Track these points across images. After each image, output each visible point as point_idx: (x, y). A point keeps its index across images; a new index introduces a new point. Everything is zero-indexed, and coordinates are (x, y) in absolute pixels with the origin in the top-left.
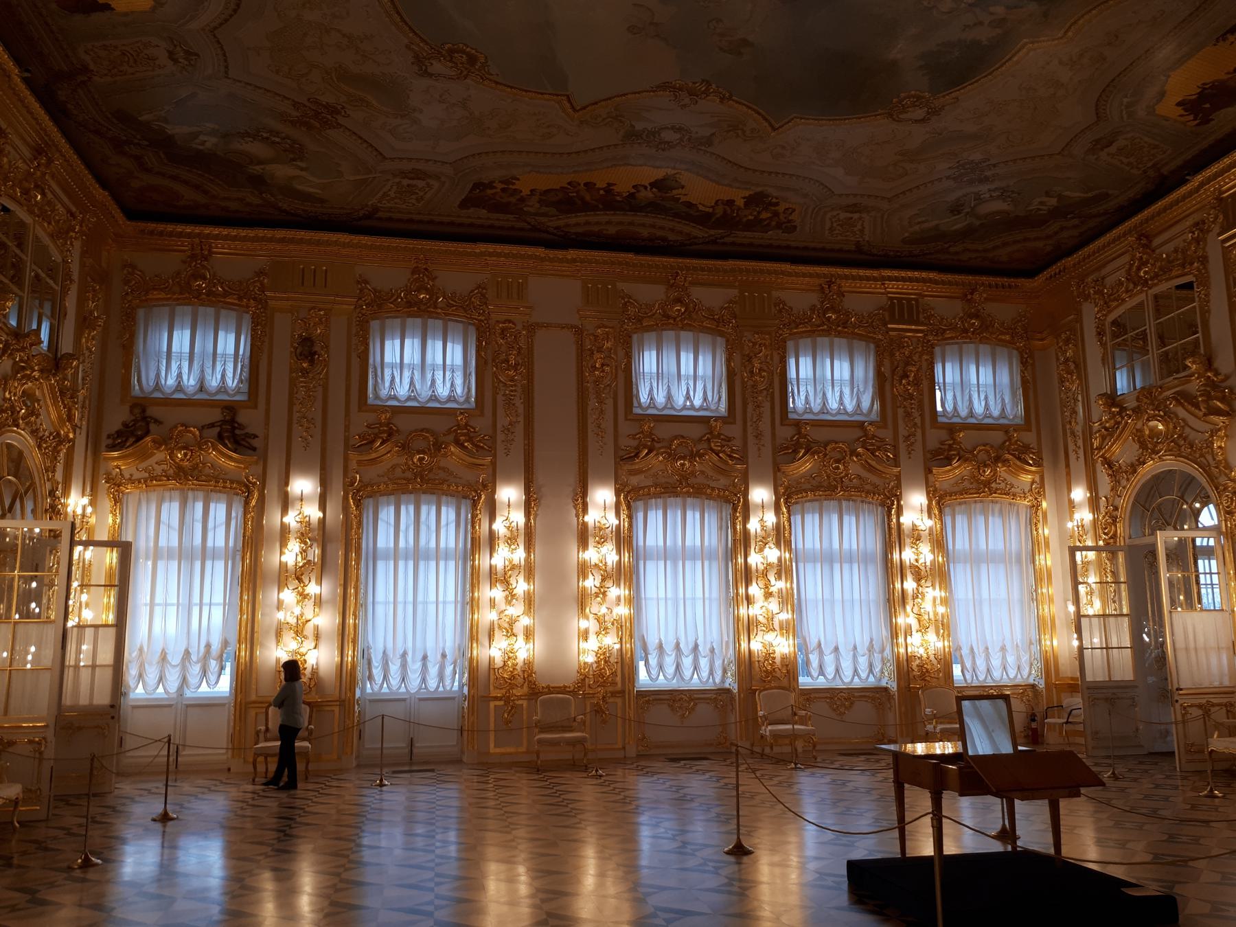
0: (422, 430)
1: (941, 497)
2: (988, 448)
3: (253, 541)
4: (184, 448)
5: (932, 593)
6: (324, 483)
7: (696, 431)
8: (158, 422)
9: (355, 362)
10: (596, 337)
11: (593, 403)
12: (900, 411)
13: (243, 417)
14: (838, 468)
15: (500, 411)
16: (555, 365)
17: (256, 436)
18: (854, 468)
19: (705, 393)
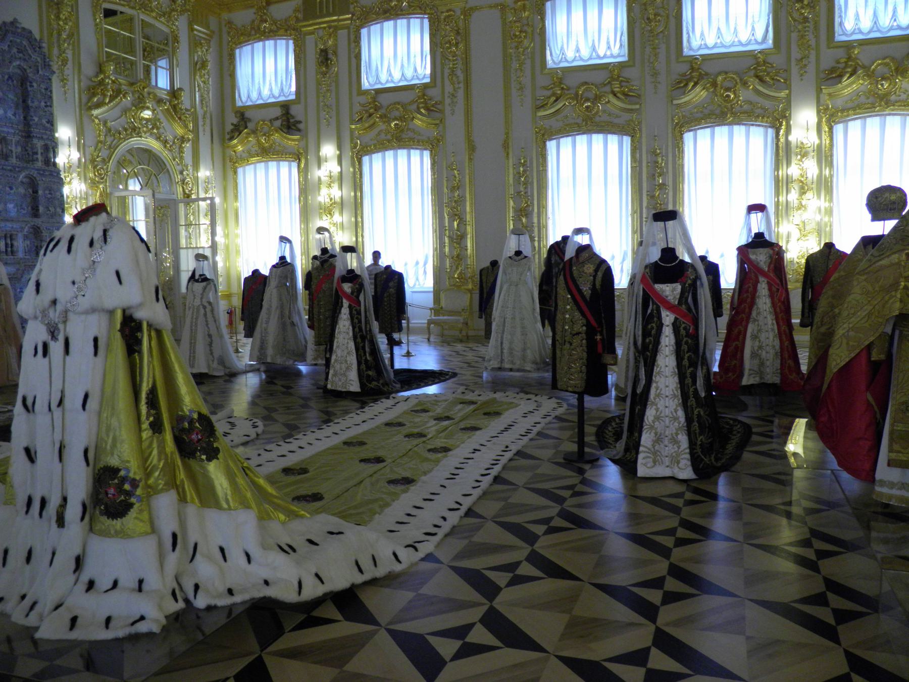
0: (395, 104)
1: (832, 115)
2: (887, 60)
3: (306, 189)
4: (264, 135)
5: (814, 202)
6: (339, 147)
7: (601, 77)
8: (250, 120)
9: (354, 61)
10: (515, 10)
11: (516, 65)
12: (794, 35)
13: (294, 110)
14: (728, 96)
15: (447, 82)
16: (486, 35)
17: (300, 122)
18: (744, 95)
19: (608, 43)
